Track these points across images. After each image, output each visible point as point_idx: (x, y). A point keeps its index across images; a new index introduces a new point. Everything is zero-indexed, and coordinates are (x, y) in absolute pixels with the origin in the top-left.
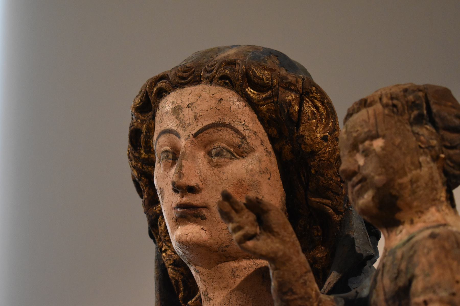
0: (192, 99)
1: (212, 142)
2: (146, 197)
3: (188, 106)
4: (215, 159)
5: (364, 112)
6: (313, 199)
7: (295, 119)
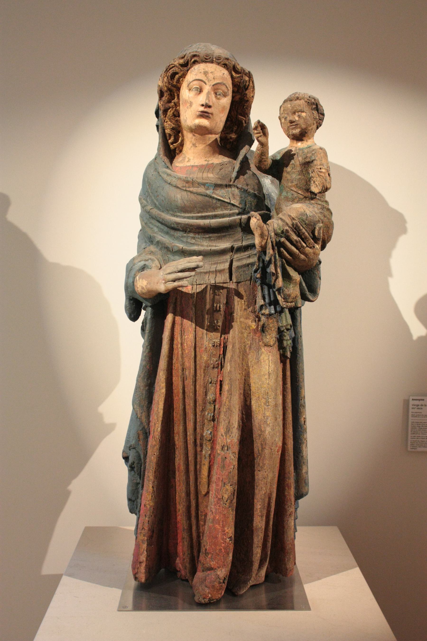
2: (166, 99)
3: (211, 73)
4: (218, 97)
5: (298, 101)
6: (240, 117)
7: (246, 87)
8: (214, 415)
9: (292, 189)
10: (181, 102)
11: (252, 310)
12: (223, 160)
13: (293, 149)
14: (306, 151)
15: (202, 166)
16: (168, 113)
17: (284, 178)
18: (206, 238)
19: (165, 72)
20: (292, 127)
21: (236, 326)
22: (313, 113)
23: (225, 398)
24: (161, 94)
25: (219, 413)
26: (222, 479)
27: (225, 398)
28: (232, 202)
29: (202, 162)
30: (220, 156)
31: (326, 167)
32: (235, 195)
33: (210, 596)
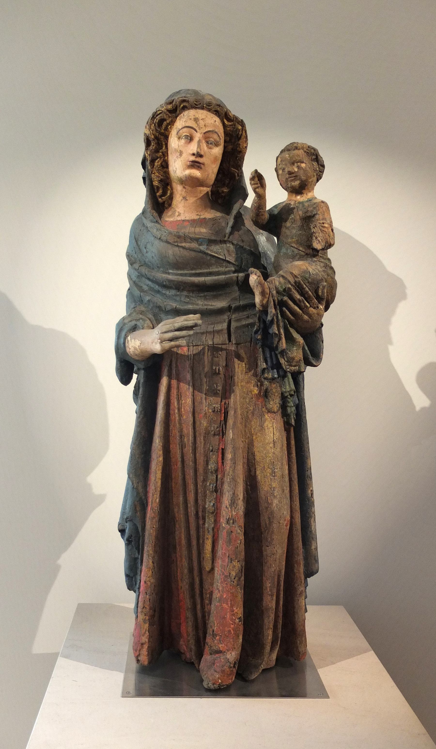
0: (203, 117)
1: (209, 137)
2: (154, 148)
5: (296, 152)
6: (232, 169)
7: (239, 137)
8: (216, 485)
9: (292, 245)
10: (169, 152)
11: (253, 374)
12: (216, 215)
13: (292, 203)
14: (306, 204)
15: (194, 221)
16: (156, 164)
17: (282, 233)
18: (200, 297)
19: (151, 119)
20: (291, 179)
21: (238, 391)
22: (313, 164)
23: (228, 467)
24: (148, 143)
25: (222, 484)
26: (229, 554)
27: (228, 467)
28: (227, 259)
29: (194, 216)
30: (212, 210)
31: (329, 222)
32: (230, 251)
33: (220, 681)
